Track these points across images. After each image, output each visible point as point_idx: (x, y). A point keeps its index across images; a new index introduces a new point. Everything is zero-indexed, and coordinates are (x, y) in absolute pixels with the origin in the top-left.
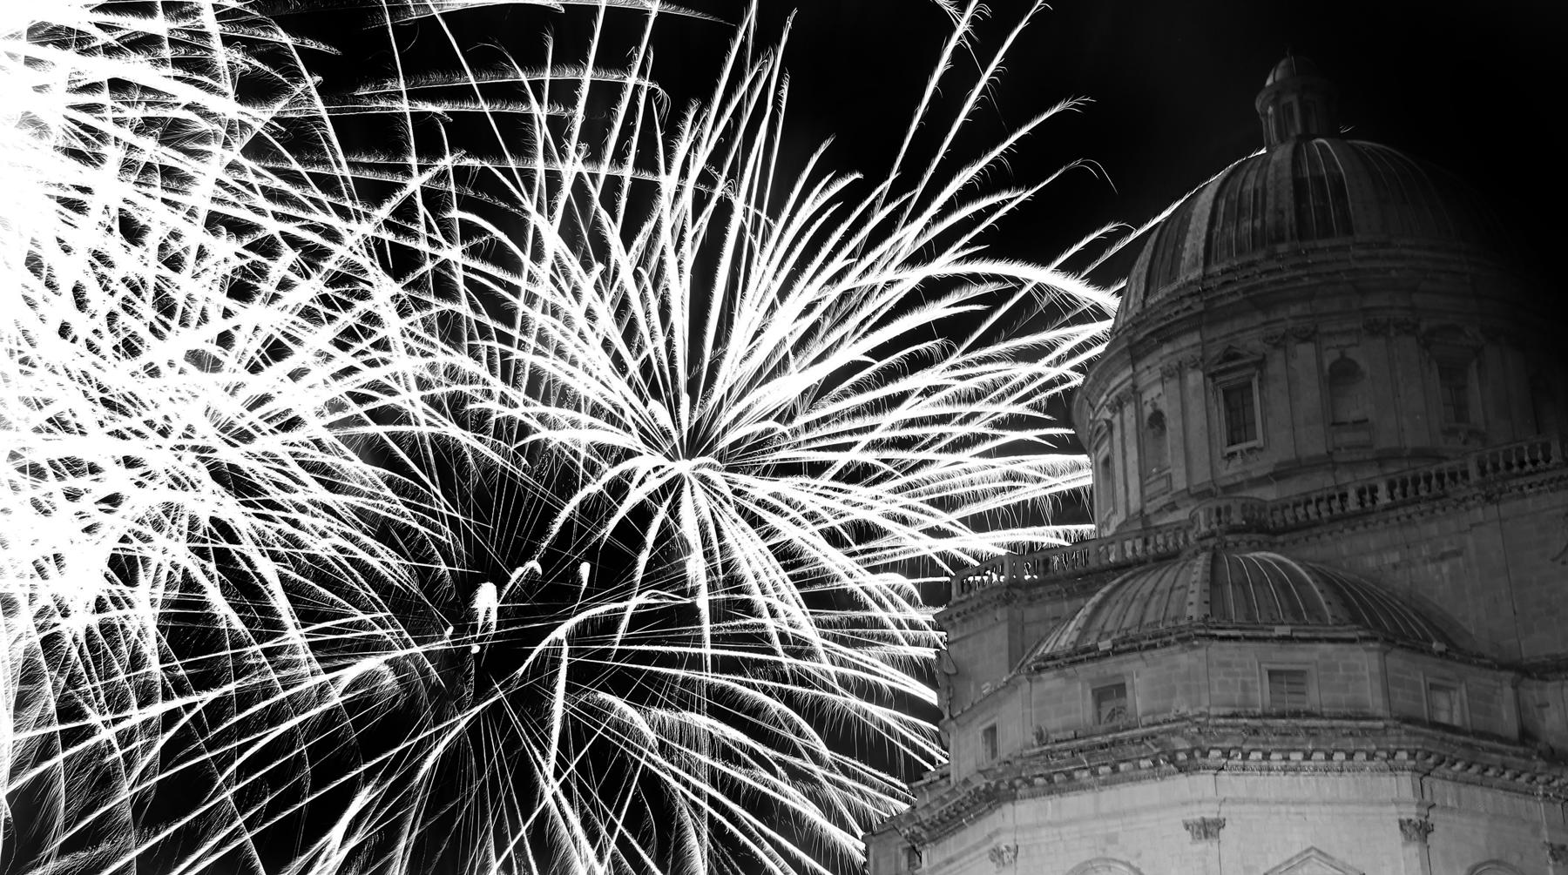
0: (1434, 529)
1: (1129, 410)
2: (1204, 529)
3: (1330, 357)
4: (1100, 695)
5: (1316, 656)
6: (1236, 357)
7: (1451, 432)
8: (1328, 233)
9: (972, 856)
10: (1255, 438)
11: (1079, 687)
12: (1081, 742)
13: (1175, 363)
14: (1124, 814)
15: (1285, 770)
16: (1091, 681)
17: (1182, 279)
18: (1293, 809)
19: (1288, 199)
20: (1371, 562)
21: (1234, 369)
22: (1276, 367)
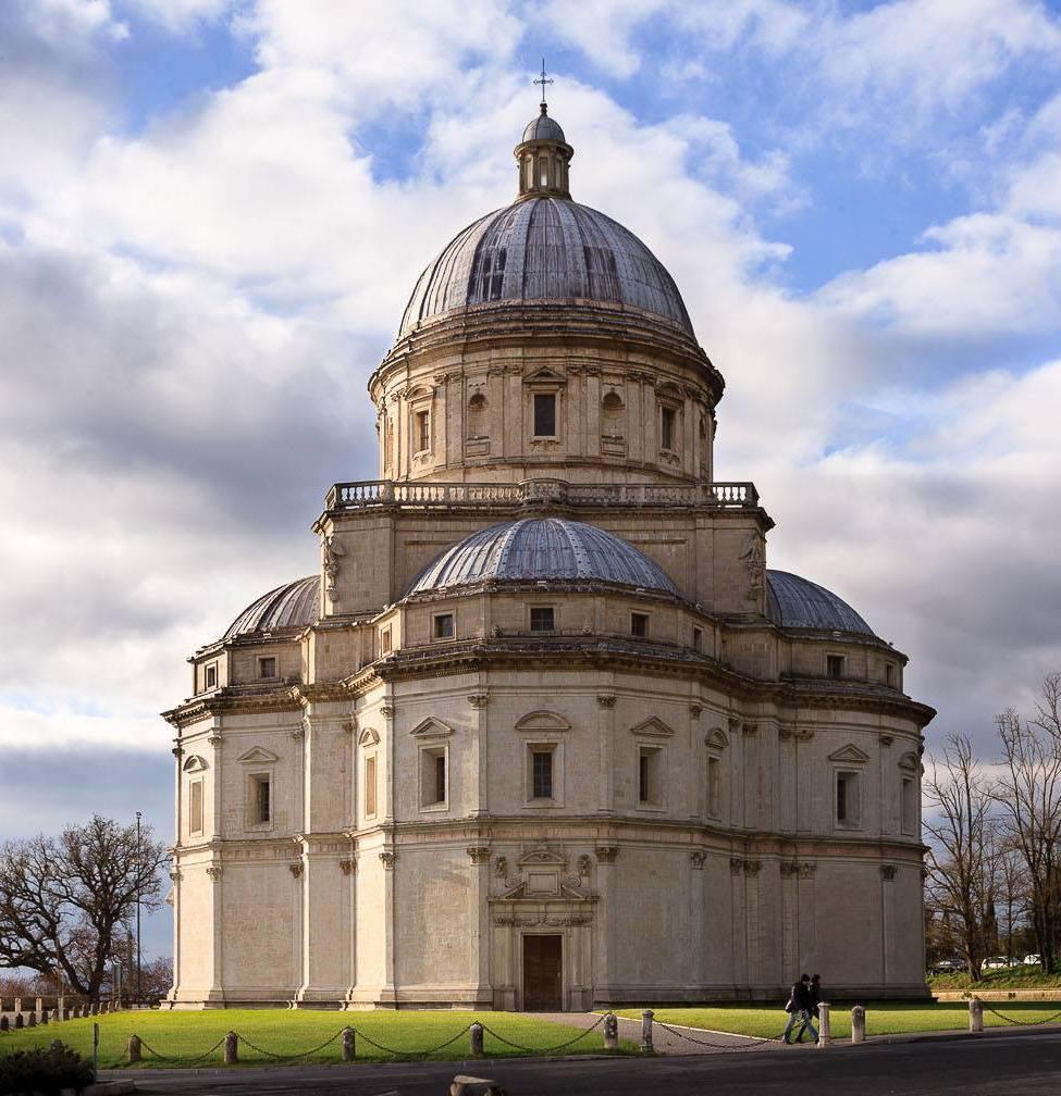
1: (454, 387)
2: (532, 496)
3: (606, 390)
4: (535, 613)
6: (548, 375)
7: (665, 455)
9: (442, 695)
10: (553, 434)
11: (523, 605)
13: (501, 366)
14: (560, 687)
16: (531, 604)
17: (504, 302)
18: (646, 695)
20: (631, 536)
22: (573, 388)
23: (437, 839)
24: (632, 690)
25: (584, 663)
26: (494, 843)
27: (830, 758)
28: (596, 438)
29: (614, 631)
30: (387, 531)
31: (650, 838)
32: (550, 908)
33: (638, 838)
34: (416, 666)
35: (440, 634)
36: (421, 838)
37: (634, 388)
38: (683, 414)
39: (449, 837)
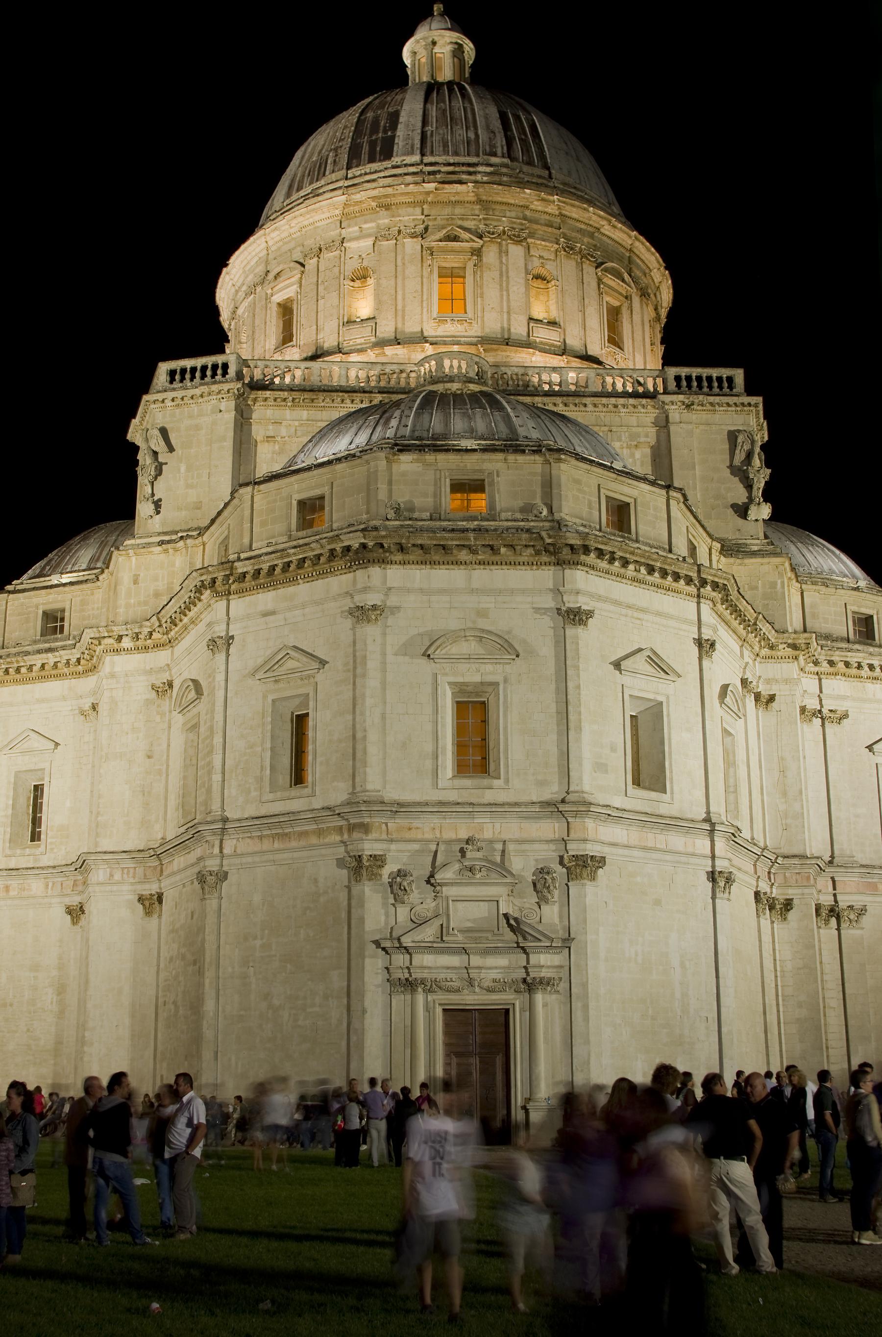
0: (633, 420)
5: (635, 493)
6: (456, 239)
8: (530, 163)
12: (445, 523)
15: (634, 580)
18: (636, 614)
19: (497, 124)
21: (453, 251)
22: (491, 255)
23: (294, 844)
24: (616, 603)
25: (538, 553)
26: (393, 847)
27: (870, 748)
28: (524, 320)
29: (582, 519)
30: (230, 416)
31: (650, 844)
32: (491, 961)
33: (632, 842)
34: (265, 567)
35: (305, 523)
36: (266, 845)
37: (569, 266)
38: (631, 308)
39: (314, 840)
